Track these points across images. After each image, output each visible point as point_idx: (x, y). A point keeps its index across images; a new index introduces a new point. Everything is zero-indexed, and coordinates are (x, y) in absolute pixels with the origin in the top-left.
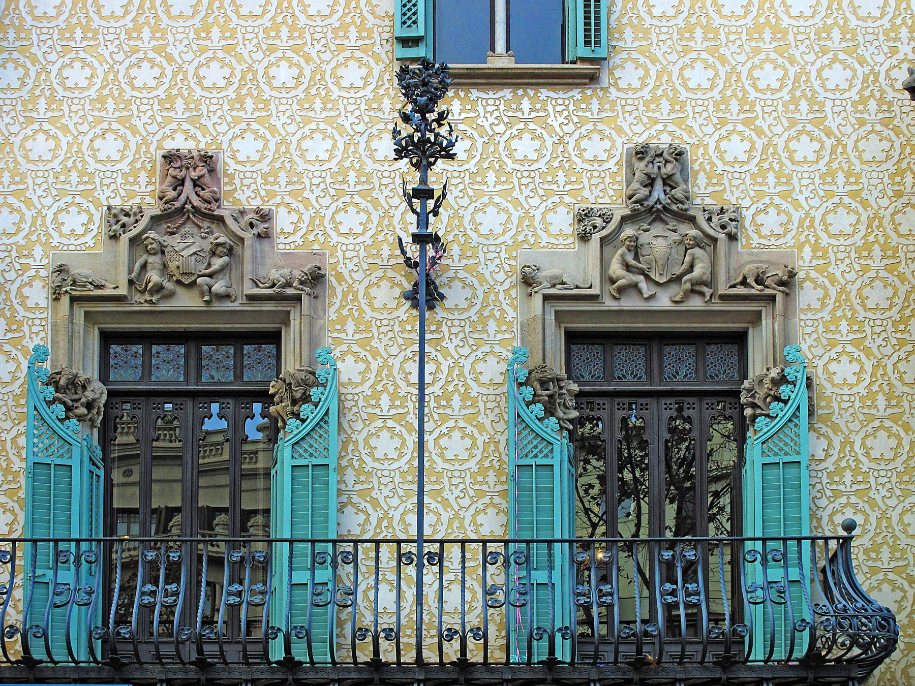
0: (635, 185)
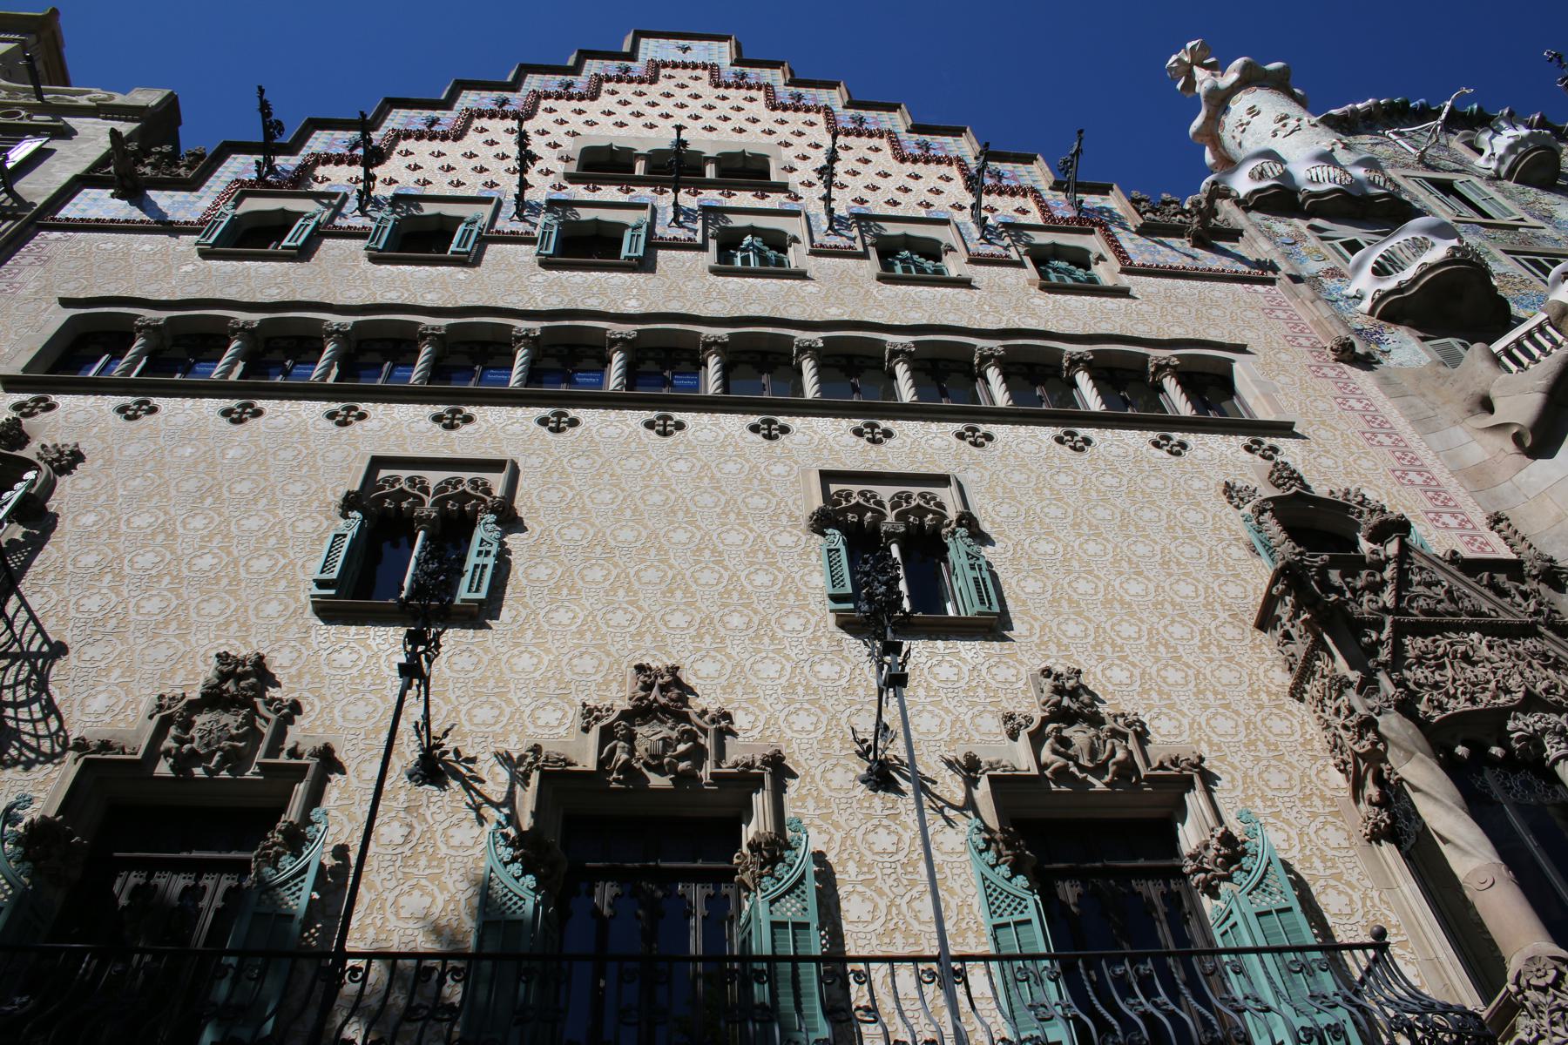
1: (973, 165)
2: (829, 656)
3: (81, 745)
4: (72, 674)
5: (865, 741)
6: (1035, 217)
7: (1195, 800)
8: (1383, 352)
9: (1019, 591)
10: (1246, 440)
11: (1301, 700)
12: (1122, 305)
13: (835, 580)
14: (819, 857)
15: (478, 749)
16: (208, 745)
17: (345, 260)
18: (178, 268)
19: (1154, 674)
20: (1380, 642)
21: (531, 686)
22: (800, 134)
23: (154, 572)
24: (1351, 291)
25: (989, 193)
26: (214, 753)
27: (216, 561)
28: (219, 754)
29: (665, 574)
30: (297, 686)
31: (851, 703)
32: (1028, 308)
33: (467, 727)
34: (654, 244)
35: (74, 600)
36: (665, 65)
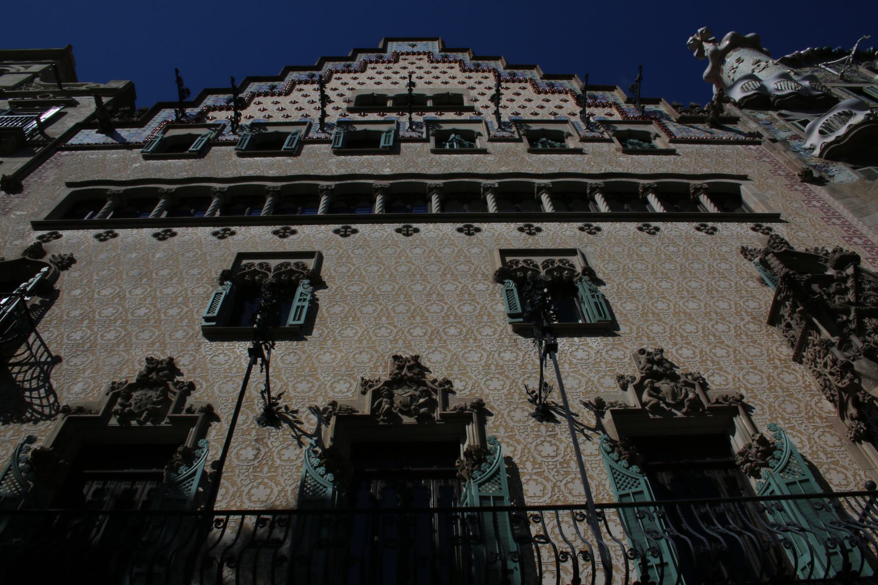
1: (579, 92)
2: (509, 348)
3: (66, 410)
4: (64, 373)
5: (533, 392)
6: (617, 116)
7: (740, 421)
8: (830, 176)
9: (622, 309)
10: (752, 225)
11: (801, 362)
12: (672, 159)
13: (511, 306)
14: (508, 460)
15: (299, 405)
16: (140, 407)
17: (224, 156)
18: (131, 165)
19: (708, 352)
20: (849, 321)
21: (331, 370)
22: (480, 83)
23: (112, 318)
24: (807, 145)
25: (590, 106)
26: (142, 413)
27: (148, 311)
28: (146, 412)
29: (410, 308)
30: (193, 375)
31: (524, 373)
32: (617, 162)
33: (293, 394)
34: (399, 140)
35: (66, 334)
36: (403, 54)
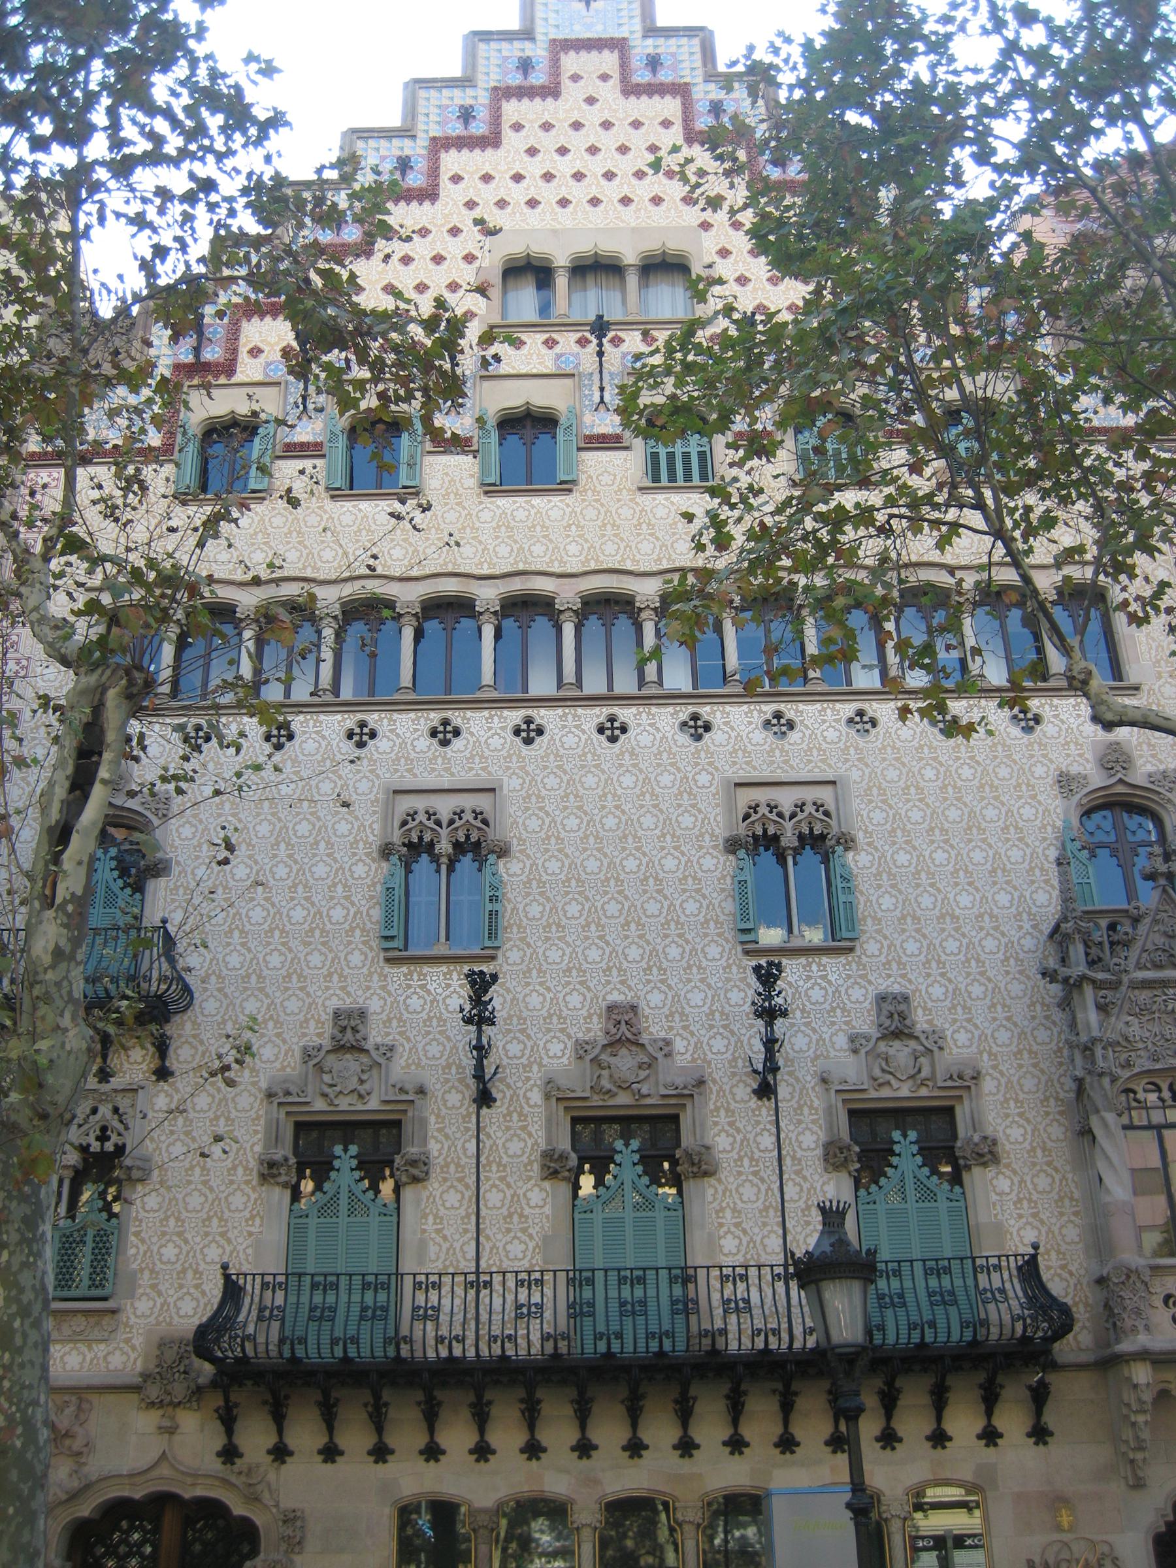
0: (883, 1018)
33: (505, 1061)
